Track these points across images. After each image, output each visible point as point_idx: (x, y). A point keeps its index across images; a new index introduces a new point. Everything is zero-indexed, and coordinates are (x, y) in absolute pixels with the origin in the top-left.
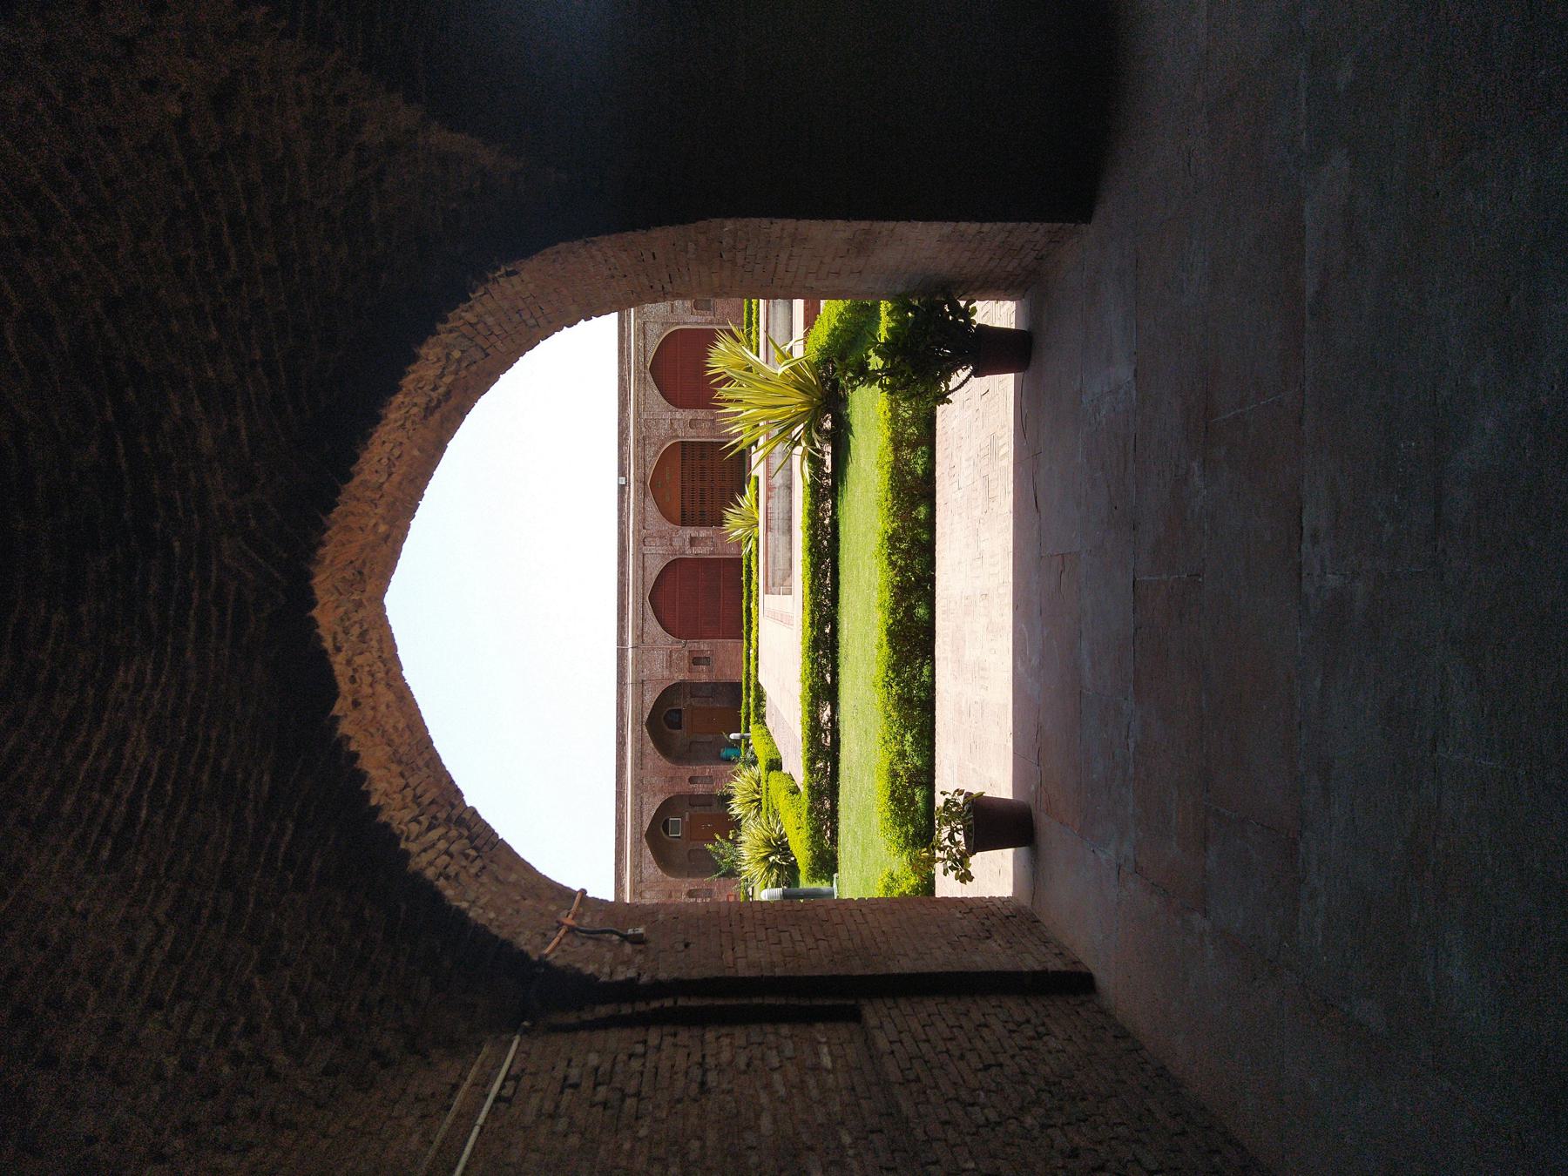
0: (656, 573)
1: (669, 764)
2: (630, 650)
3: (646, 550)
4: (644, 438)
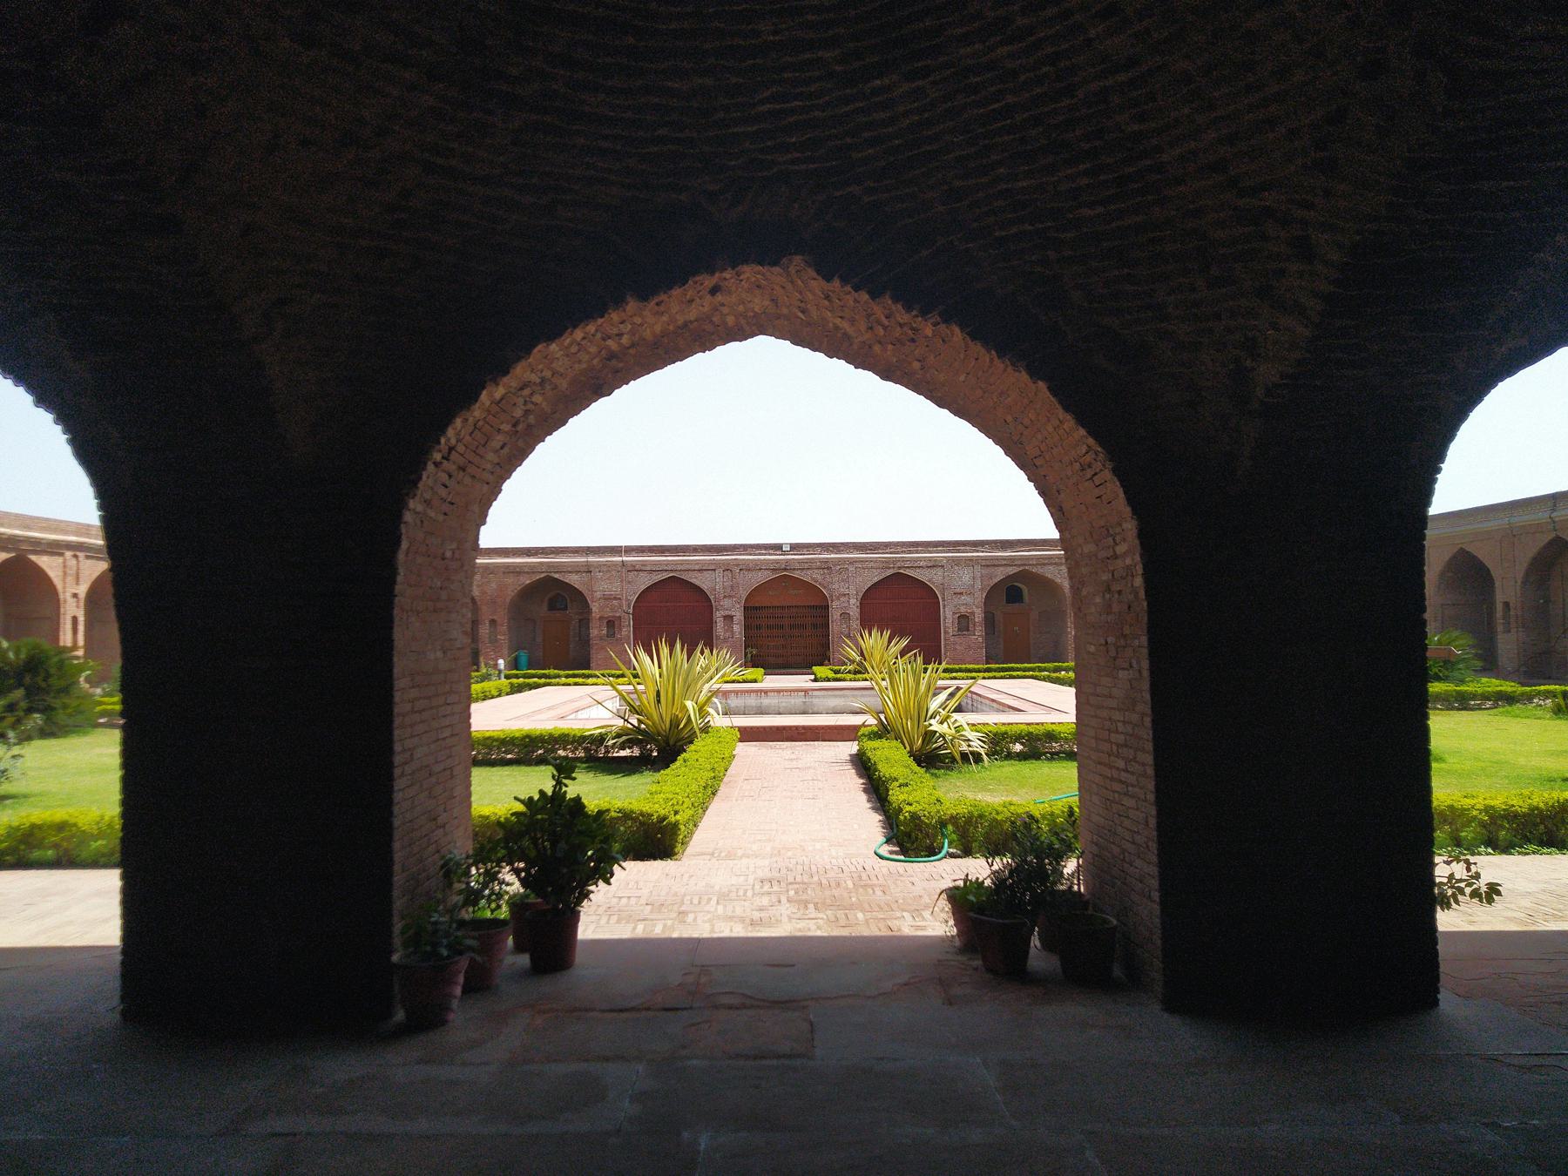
0: (697, 582)
1: (508, 600)
2: (620, 559)
3: (719, 572)
4: (830, 568)
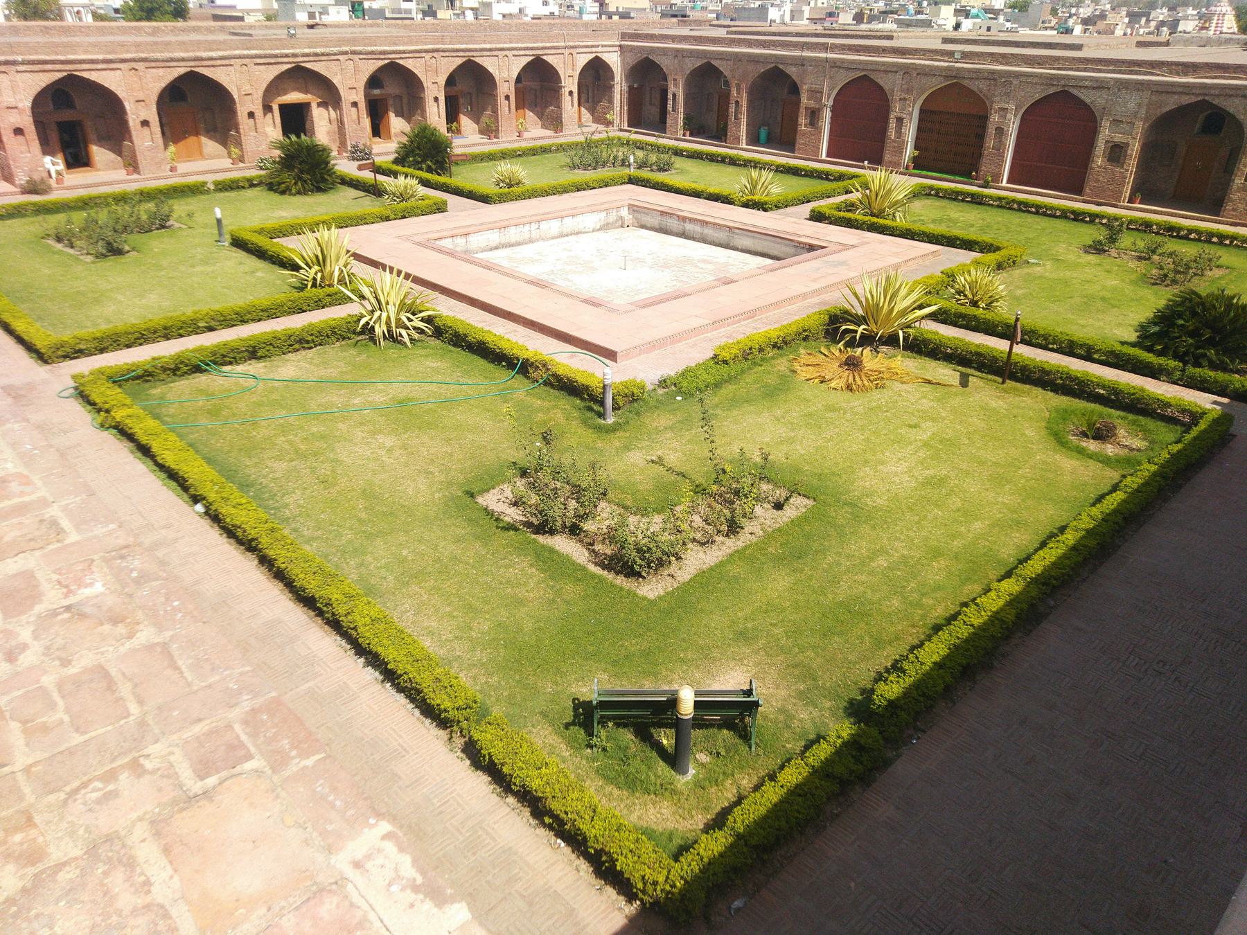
0: (881, 83)
3: (899, 76)
